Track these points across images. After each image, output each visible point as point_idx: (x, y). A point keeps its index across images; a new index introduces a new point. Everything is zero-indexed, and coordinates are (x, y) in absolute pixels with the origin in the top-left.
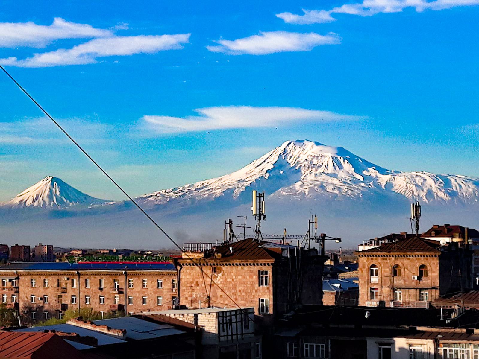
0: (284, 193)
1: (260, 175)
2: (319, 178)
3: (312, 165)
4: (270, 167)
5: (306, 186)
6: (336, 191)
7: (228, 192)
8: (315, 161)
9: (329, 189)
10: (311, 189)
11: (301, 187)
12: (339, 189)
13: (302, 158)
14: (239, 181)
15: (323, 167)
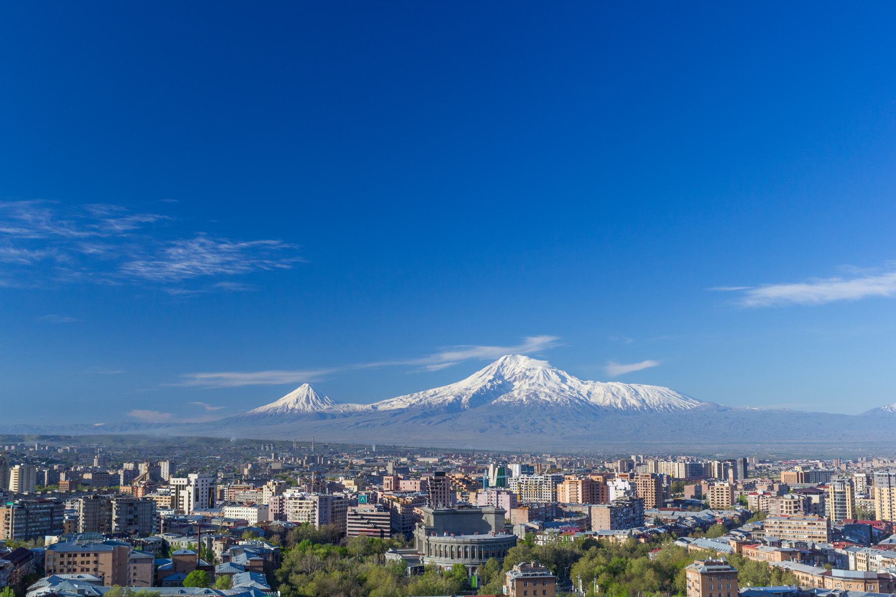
0: (505, 400)
1: (484, 384)
2: (533, 387)
3: (525, 376)
4: (491, 377)
5: (523, 394)
6: (548, 399)
7: (458, 399)
8: (528, 373)
9: (542, 397)
10: (528, 397)
11: (519, 394)
12: (550, 397)
13: (517, 371)
14: (466, 389)
15: (535, 378)
